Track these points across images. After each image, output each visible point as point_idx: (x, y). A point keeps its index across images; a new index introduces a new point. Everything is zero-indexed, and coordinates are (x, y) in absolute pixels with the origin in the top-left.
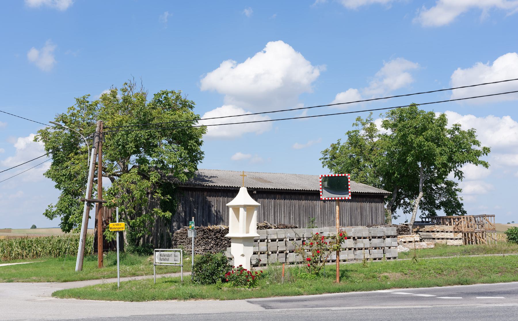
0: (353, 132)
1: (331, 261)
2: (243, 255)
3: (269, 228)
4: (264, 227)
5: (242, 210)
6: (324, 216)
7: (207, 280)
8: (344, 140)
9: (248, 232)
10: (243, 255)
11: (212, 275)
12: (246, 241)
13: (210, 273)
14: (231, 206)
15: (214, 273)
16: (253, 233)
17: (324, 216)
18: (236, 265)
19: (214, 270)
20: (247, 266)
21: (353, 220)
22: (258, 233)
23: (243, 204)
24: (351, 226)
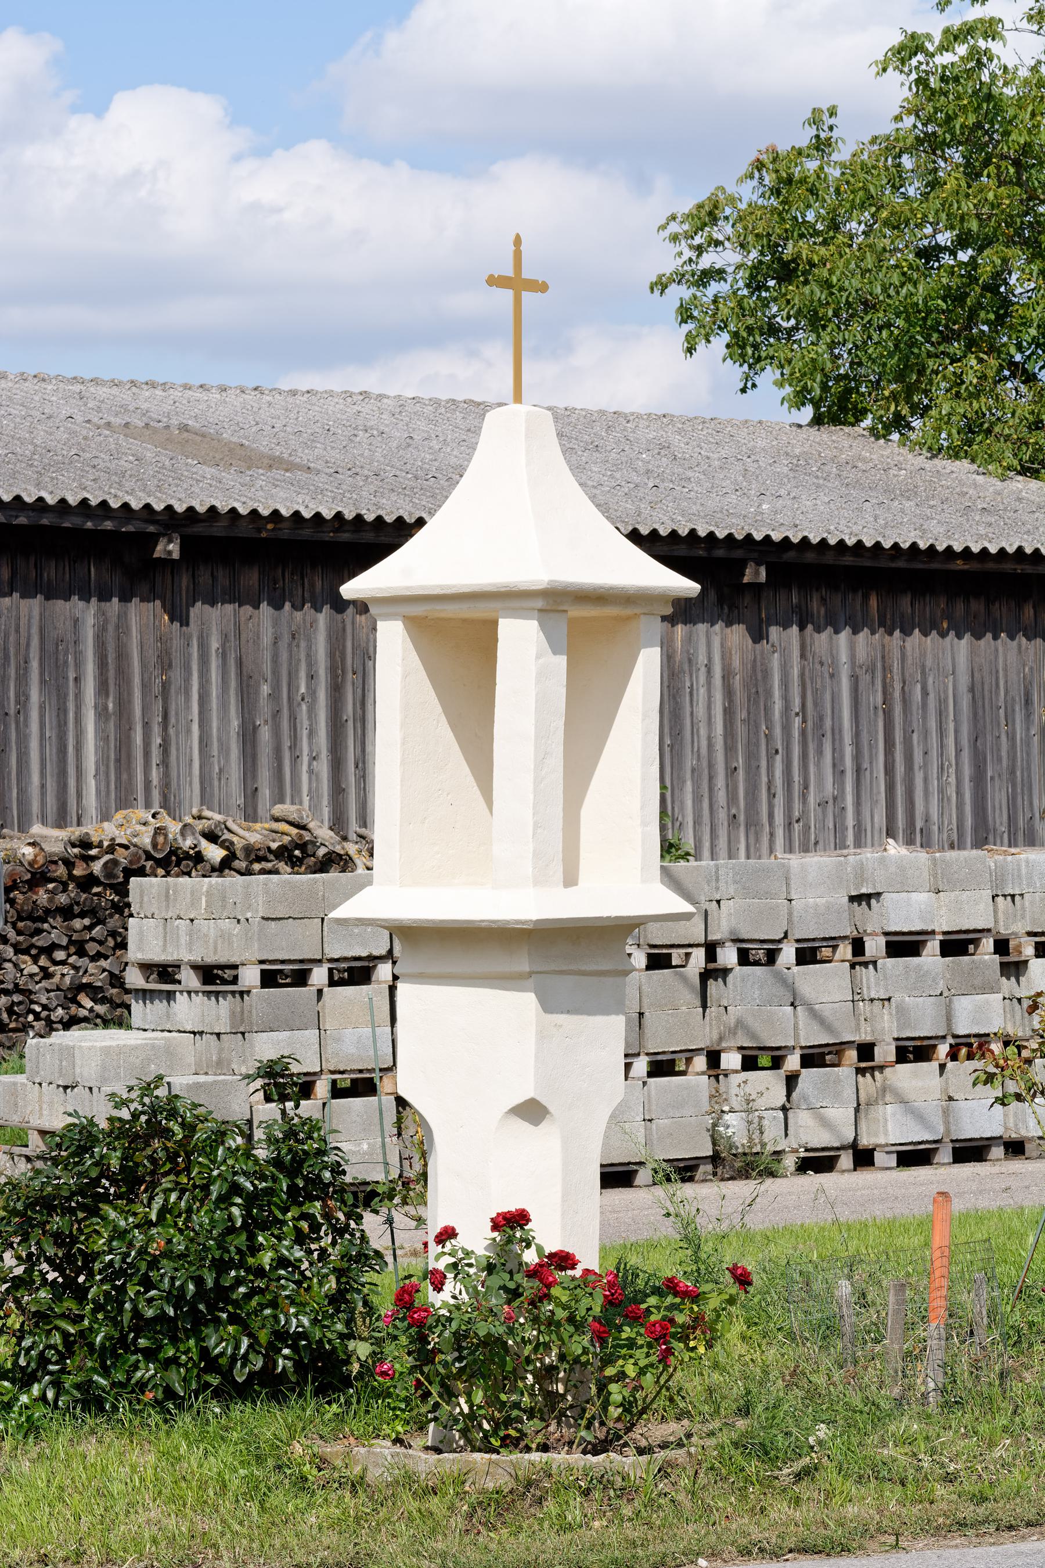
0: (953, 37)
1: (945, 1155)
2: (532, 1111)
3: (323, 866)
4: (284, 853)
5: (520, 640)
6: (751, 756)
7: (147, 1371)
8: (878, 106)
9: (247, 887)
10: (532, 1111)
11: (198, 1323)
12: (564, 956)
13: (177, 1297)
14: (396, 603)
15: (222, 1294)
16: (624, 880)
17: (751, 756)
18: (462, 1203)
19: (221, 1266)
20: (572, 1224)
21: (998, 797)
22: (670, 879)
23: (536, 572)
24: (980, 843)
